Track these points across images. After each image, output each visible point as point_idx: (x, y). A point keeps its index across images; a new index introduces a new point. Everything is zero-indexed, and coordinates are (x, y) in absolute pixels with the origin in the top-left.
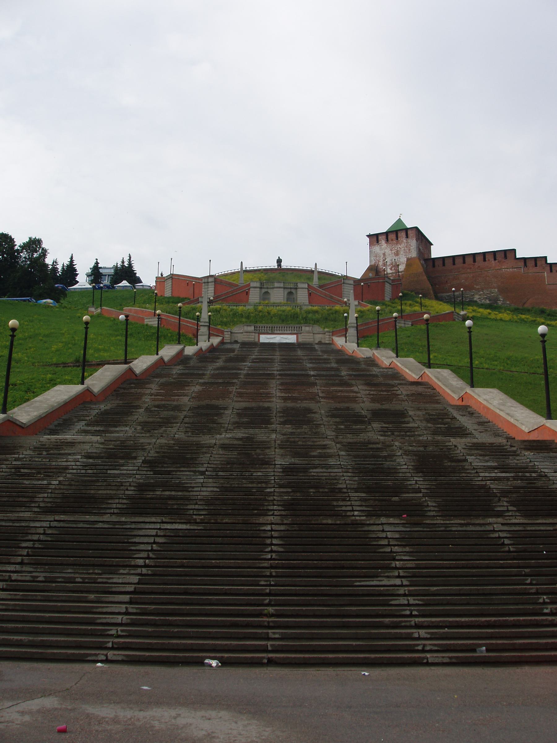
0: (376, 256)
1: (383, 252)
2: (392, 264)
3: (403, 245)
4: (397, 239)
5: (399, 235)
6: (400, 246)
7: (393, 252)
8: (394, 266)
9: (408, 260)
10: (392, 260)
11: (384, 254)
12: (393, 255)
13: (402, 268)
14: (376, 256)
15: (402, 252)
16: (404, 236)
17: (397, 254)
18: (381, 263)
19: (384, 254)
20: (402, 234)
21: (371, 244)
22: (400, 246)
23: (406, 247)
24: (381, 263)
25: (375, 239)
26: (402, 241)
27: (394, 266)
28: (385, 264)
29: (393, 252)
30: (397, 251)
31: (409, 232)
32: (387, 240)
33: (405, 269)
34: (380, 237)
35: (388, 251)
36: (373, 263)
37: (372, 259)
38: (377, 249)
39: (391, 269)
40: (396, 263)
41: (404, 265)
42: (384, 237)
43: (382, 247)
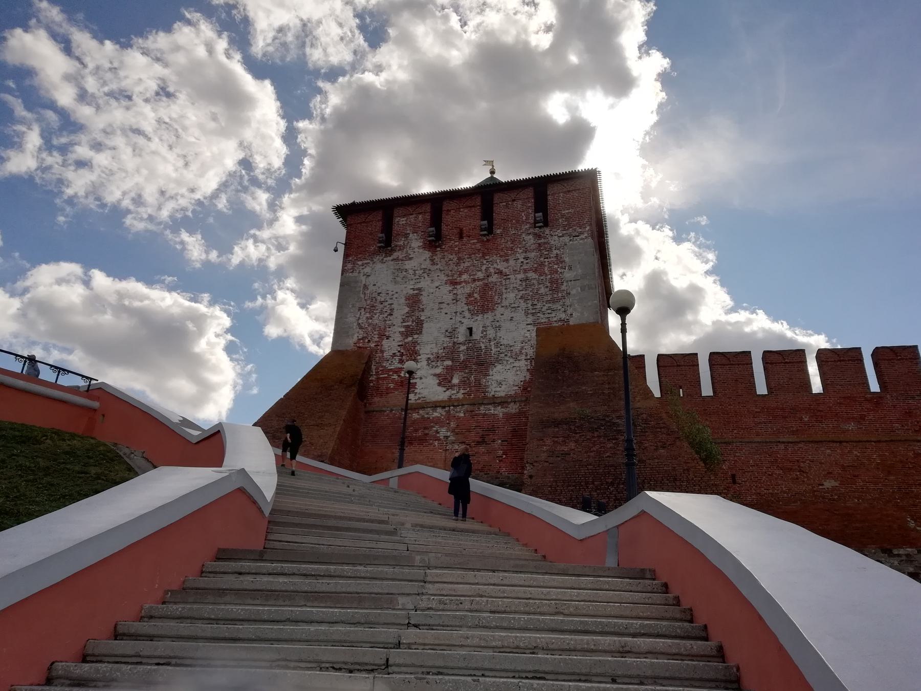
1: (408, 289)
2: (451, 352)
4: (490, 230)
5: (500, 210)
6: (501, 266)
7: (463, 291)
8: (464, 366)
9: (544, 332)
10: (451, 333)
11: (414, 301)
12: (462, 306)
13: (506, 378)
15: (511, 296)
17: (484, 302)
18: (391, 346)
19: (414, 301)
20: (518, 204)
21: (353, 250)
22: (501, 266)
23: (538, 269)
24: (391, 346)
25: (376, 222)
27: (464, 366)
28: (411, 352)
29: (463, 291)
30: (486, 289)
32: (434, 242)
33: (526, 387)
34: (400, 221)
35: (435, 289)
36: (350, 343)
37: (351, 319)
38: (379, 274)
39: (444, 380)
41: (523, 364)
42: (422, 218)
43: (409, 265)
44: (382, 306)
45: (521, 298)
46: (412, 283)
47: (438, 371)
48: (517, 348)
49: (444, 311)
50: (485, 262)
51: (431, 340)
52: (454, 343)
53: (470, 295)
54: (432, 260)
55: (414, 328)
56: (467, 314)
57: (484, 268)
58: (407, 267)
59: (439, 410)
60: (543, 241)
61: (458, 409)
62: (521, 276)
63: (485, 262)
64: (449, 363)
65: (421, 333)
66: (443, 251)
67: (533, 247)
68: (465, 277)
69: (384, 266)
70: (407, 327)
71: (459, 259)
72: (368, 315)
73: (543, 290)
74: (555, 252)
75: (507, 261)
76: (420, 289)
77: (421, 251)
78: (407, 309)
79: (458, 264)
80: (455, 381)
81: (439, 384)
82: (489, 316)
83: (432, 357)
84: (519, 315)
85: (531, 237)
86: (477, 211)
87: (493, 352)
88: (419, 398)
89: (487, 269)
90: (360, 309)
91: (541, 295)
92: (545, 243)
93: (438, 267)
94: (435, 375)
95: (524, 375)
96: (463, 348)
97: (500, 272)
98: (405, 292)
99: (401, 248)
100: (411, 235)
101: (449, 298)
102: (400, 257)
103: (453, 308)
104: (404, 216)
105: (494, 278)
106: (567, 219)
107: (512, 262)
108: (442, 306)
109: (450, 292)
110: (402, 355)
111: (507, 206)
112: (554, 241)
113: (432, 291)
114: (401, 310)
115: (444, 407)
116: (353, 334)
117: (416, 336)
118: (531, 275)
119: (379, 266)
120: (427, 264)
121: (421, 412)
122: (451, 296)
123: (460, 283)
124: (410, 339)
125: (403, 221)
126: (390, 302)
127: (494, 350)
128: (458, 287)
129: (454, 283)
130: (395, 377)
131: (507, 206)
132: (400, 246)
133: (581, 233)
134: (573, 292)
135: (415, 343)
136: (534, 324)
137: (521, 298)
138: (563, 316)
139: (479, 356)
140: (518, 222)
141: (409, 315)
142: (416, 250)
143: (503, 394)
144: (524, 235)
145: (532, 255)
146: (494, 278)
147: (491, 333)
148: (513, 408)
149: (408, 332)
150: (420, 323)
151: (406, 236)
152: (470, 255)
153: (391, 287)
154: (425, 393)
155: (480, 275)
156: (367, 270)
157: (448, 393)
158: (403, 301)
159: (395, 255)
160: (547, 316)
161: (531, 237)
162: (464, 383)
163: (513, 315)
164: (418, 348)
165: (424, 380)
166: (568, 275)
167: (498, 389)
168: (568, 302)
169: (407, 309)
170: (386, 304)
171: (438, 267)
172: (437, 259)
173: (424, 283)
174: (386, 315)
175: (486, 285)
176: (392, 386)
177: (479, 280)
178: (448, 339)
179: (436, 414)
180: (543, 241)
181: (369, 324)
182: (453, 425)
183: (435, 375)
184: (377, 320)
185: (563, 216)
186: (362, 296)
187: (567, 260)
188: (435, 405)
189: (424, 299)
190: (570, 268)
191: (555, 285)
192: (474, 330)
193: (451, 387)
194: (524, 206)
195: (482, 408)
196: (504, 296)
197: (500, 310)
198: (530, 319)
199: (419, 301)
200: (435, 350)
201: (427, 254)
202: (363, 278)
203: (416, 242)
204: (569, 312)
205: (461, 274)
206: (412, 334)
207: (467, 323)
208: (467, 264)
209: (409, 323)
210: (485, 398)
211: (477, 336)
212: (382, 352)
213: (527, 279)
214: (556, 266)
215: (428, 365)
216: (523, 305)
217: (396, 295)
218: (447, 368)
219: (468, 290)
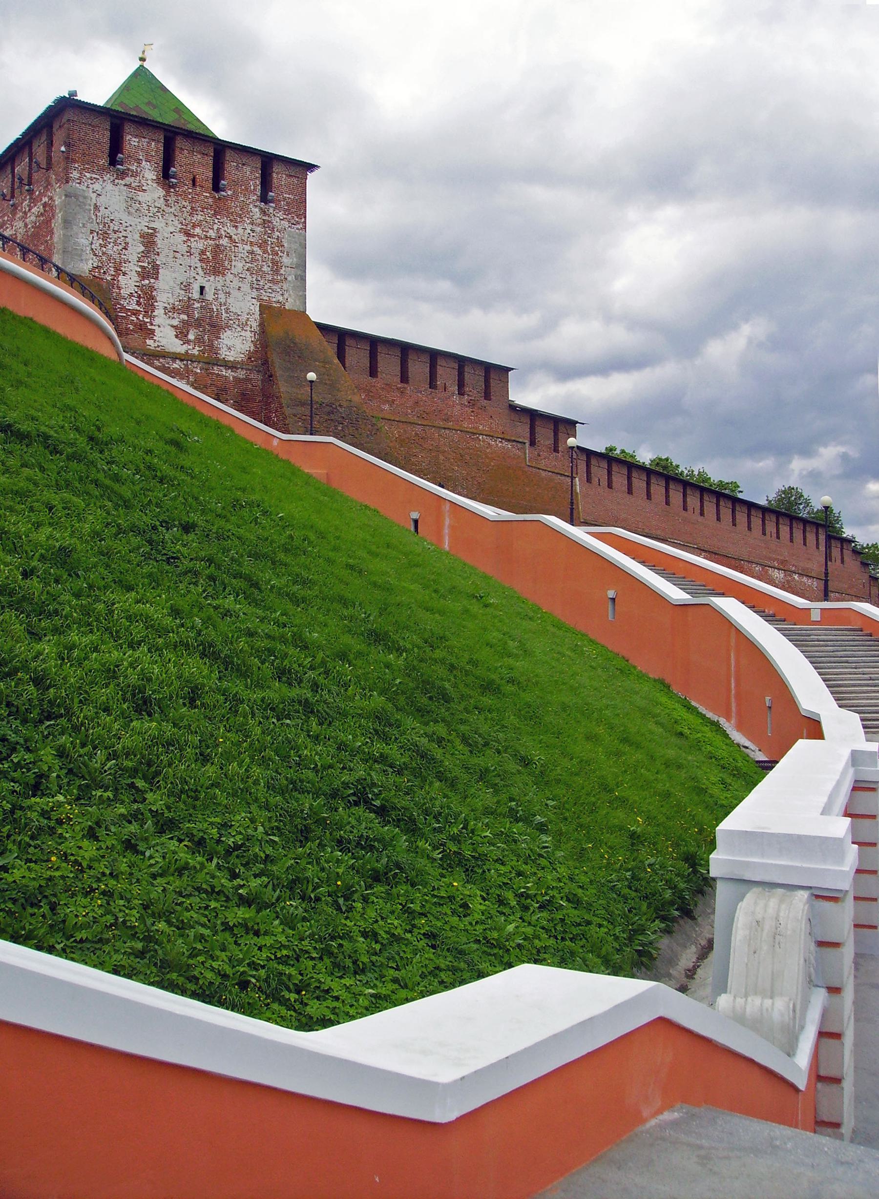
0: (105, 236)
1: (142, 224)
2: (186, 307)
6: (232, 231)
7: (198, 245)
8: (198, 324)
9: (265, 309)
11: (149, 240)
12: (195, 261)
13: (236, 344)
14: (105, 236)
15: (239, 266)
16: (255, 184)
17: (215, 263)
19: (149, 240)
20: (247, 170)
22: (232, 231)
23: (263, 245)
26: (245, 210)
27: (198, 324)
28: (148, 298)
30: (217, 250)
31: (279, 176)
35: (169, 233)
39: (181, 334)
40: (206, 308)
42: (156, 147)
43: (142, 197)
44: (116, 236)
45: (248, 270)
46: (147, 219)
47: (175, 322)
48: (243, 318)
49: (179, 261)
50: (216, 221)
51: (167, 289)
52: (189, 298)
53: (203, 252)
54: (167, 201)
55: (150, 272)
56: (200, 270)
57: (215, 227)
58: (140, 198)
59: (178, 361)
60: (266, 218)
61: (195, 364)
62: (248, 248)
63: (216, 221)
64: (185, 317)
65: (157, 278)
66: (177, 194)
67: (259, 221)
68: (198, 231)
69: (116, 188)
70: (143, 267)
71: (192, 208)
72: (101, 241)
73: (265, 269)
74: (277, 233)
75: (236, 227)
76: (154, 229)
77: (155, 185)
78: (143, 248)
79: (191, 214)
80: (191, 337)
81: (177, 336)
82: (220, 278)
83: (168, 307)
84: (246, 287)
85: (257, 210)
86: (210, 161)
87: (223, 316)
88: (158, 346)
89: (218, 229)
90: (92, 232)
91: (264, 272)
92: (269, 222)
93: (172, 210)
94: (172, 326)
95: (248, 346)
96: (197, 305)
97: (231, 237)
98: (139, 228)
99: (135, 174)
100: (144, 163)
102: (133, 185)
103: (187, 261)
104: (136, 136)
105: (225, 242)
106: (288, 204)
107: (240, 231)
108: (177, 255)
109: (185, 242)
110: (139, 297)
111: (237, 168)
112: (276, 222)
113: (166, 235)
114: (136, 248)
115: (182, 360)
116: (87, 260)
117: (152, 281)
118: (256, 249)
119: (109, 186)
120: (161, 203)
121: (161, 360)
122: (183, 248)
123: (193, 236)
124: (147, 282)
125: (135, 141)
126: (124, 233)
127: (224, 315)
128: (192, 240)
129: (188, 234)
130: (133, 318)
131: (237, 168)
132: (132, 171)
133: (298, 223)
134: (289, 278)
135: (152, 288)
136: (259, 299)
137: (248, 270)
138: (281, 299)
139: (212, 316)
140: (246, 189)
141: (146, 254)
142: (149, 182)
143: (232, 359)
144: (251, 206)
145: (258, 229)
146: (225, 242)
147: (222, 296)
148: (241, 374)
149: (144, 274)
150: (156, 268)
151: (139, 161)
152: (203, 208)
153: (124, 217)
154: (163, 342)
155: (212, 233)
156: (97, 186)
157: (185, 347)
158: (137, 236)
159: (128, 180)
160: (268, 294)
161: (257, 210)
162: (199, 341)
163: (240, 284)
164: (154, 293)
165: (162, 329)
166: (286, 260)
167: (228, 353)
168: (285, 288)
169: (143, 248)
170: (121, 235)
171: (172, 210)
172: (172, 199)
173: (158, 224)
174: (120, 247)
175: (218, 246)
176: (131, 327)
177: (211, 239)
178: (183, 292)
179: (175, 366)
180: (266, 218)
181: (104, 253)
182: (191, 379)
183: (172, 326)
184: (111, 250)
185: (285, 199)
186: (94, 217)
187: (286, 245)
188: (175, 357)
189: (158, 240)
190: (288, 255)
191: (276, 266)
192: (207, 289)
193: (188, 342)
194: (251, 174)
195: (215, 368)
196: (233, 263)
197: (229, 277)
198: (255, 294)
199: (154, 243)
200: (171, 301)
201: (161, 192)
203: (149, 173)
204: (286, 296)
205: (194, 226)
206: (148, 277)
207: (201, 281)
208: (200, 218)
209: (146, 265)
210: (218, 359)
211: (209, 295)
212: (119, 288)
213: (252, 253)
214: (277, 248)
215: (166, 314)
216: (249, 277)
217: (129, 229)
218: (183, 321)
219: (201, 245)
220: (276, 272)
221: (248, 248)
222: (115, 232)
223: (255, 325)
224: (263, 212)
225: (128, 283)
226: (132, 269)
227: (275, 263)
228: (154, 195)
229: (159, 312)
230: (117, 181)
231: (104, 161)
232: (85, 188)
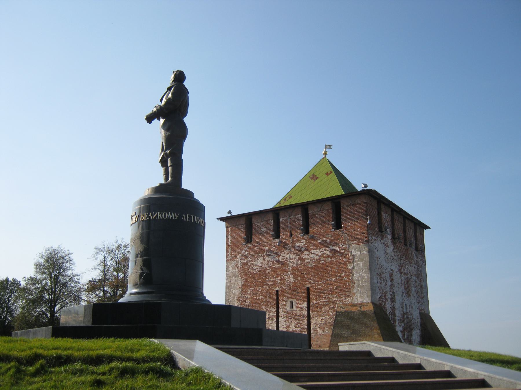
3: (412, 269)
7: (404, 278)
22: (410, 268)
30: (408, 281)
46: (390, 264)
76: (392, 270)
80: (406, 337)
101: (399, 281)
114: (389, 283)
119: (380, 245)
124: (393, 305)
129: (401, 273)
142: (389, 241)
146: (409, 275)
153: (384, 263)
155: (406, 271)
156: (376, 245)
173: (393, 268)
178: (401, 309)
202: (376, 251)
213: (415, 281)
220: (421, 291)
221: (414, 278)
222: (383, 273)
223: (419, 324)
224: (417, 257)
225: (388, 305)
226: (389, 296)
227: (421, 286)
228: (390, 249)
229: (397, 323)
230: (382, 241)
231: (377, 229)
232: (373, 246)
